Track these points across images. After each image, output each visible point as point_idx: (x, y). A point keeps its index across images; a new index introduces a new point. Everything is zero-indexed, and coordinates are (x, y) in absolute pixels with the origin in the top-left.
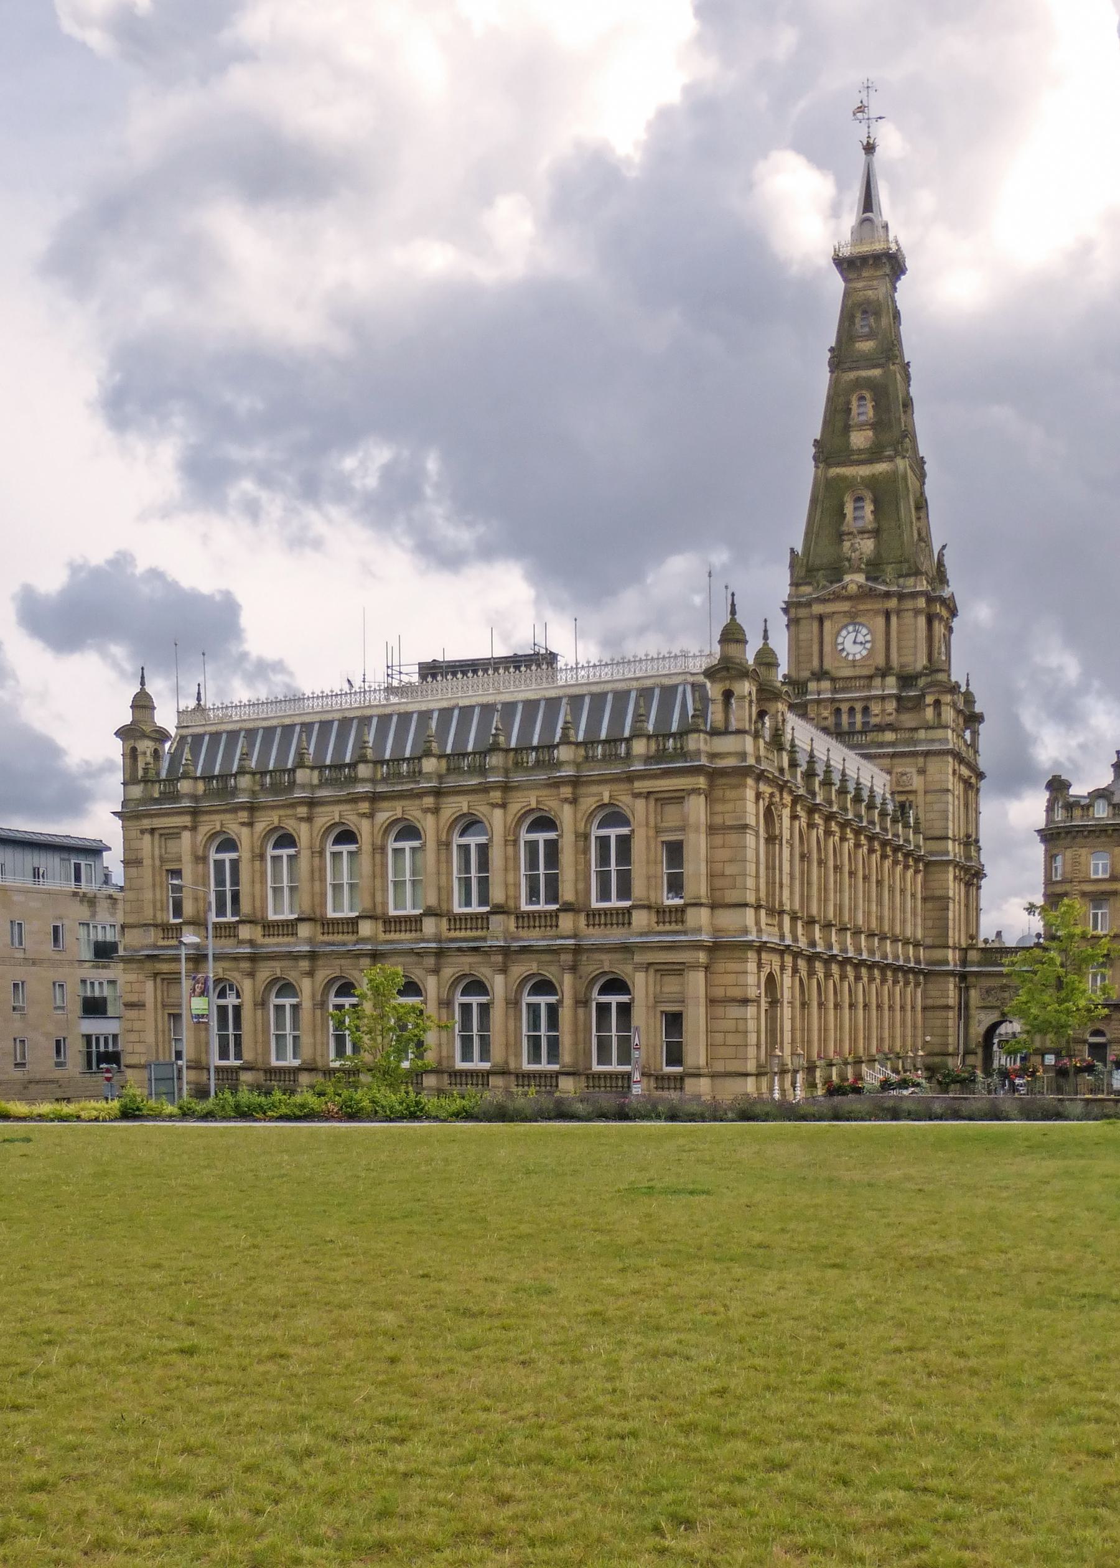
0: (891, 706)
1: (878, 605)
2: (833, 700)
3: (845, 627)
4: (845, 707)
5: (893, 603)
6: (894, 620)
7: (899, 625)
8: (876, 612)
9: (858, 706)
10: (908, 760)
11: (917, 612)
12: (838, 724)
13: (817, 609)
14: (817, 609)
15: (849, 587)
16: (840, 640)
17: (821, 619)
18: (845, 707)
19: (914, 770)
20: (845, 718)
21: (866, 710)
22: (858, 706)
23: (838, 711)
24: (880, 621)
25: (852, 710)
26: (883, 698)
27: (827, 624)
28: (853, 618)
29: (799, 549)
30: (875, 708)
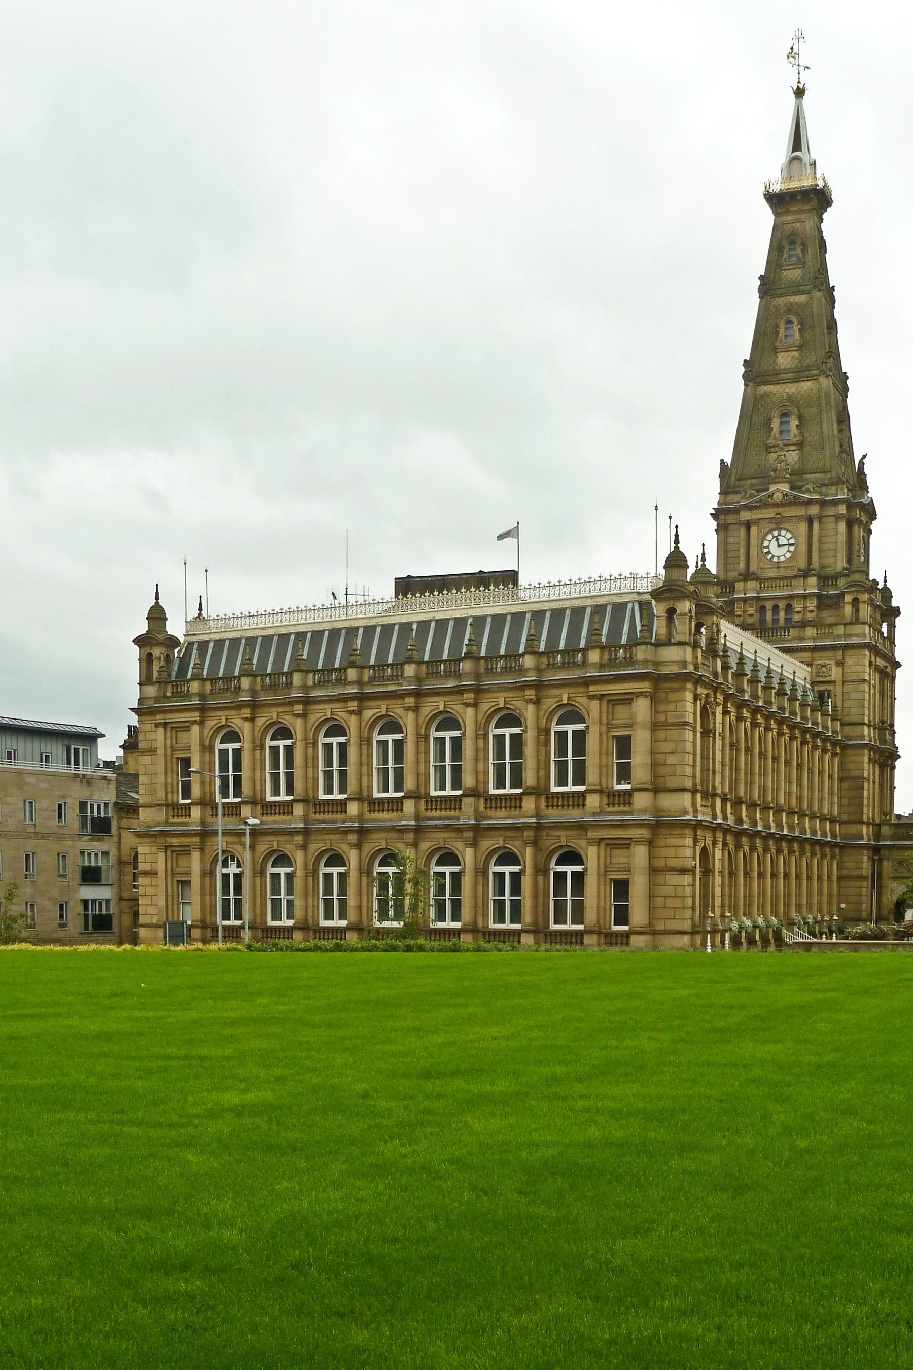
1: (801, 511)
2: (758, 599)
3: (771, 531)
4: (769, 605)
5: (814, 510)
6: (816, 525)
7: (821, 529)
8: (799, 518)
9: (782, 604)
10: (830, 653)
11: (838, 517)
12: (763, 621)
13: (745, 516)
14: (745, 516)
15: (775, 496)
17: (748, 525)
18: (769, 605)
20: (769, 615)
21: (789, 607)
22: (782, 604)
23: (763, 609)
24: (803, 527)
25: (776, 608)
26: (805, 597)
27: (754, 530)
28: (779, 523)
29: (728, 460)
30: (797, 606)
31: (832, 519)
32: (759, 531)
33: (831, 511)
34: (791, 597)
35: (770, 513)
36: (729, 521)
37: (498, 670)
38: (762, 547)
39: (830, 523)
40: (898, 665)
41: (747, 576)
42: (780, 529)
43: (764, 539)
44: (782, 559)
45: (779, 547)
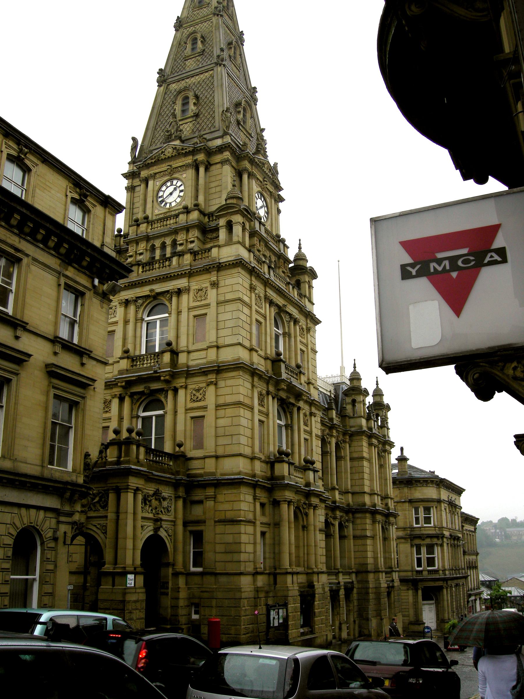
0: (195, 234)
1: (189, 160)
3: (164, 183)
5: (201, 157)
6: (202, 170)
8: (186, 167)
16: (161, 194)
18: (158, 243)
19: (208, 285)
24: (190, 173)
26: (187, 229)
27: (151, 183)
28: (171, 175)
33: (218, 158)
34: (176, 232)
35: (164, 167)
36: (135, 184)
38: (157, 197)
39: (215, 170)
40: (317, 322)
43: (159, 190)
45: (173, 195)
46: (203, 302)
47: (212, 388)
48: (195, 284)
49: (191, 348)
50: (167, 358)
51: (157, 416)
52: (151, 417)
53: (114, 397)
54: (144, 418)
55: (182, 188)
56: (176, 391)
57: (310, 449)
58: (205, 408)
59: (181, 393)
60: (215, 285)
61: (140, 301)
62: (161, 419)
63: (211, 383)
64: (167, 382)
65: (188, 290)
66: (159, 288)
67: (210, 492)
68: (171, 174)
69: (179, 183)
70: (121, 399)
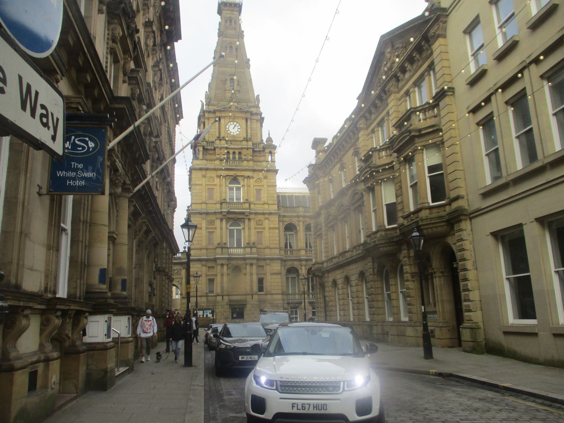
1: (243, 115)
2: (227, 148)
4: (231, 151)
5: (248, 115)
6: (249, 122)
7: (251, 125)
8: (243, 118)
9: (237, 152)
12: (228, 158)
14: (218, 114)
15: (232, 108)
16: (227, 127)
18: (231, 151)
22: (237, 152)
24: (244, 121)
25: (234, 153)
26: (247, 149)
27: (222, 121)
28: (234, 119)
30: (244, 152)
31: (255, 121)
32: (225, 122)
34: (242, 148)
37: (90, 175)
41: (219, 138)
42: (233, 121)
43: (227, 125)
44: (235, 134)
46: (261, 184)
47: (267, 221)
48: (256, 175)
49: (255, 203)
50: (247, 205)
51: (237, 230)
52: (234, 229)
53: (217, 219)
54: (230, 230)
55: (239, 127)
56: (249, 219)
57: (111, 257)
58: (264, 228)
59: (252, 222)
60: (265, 178)
61: (228, 177)
62: (239, 231)
63: (267, 219)
64: (247, 216)
65: (253, 178)
66: (239, 173)
67: (268, 262)
68: (234, 119)
69: (238, 125)
70: (222, 220)
